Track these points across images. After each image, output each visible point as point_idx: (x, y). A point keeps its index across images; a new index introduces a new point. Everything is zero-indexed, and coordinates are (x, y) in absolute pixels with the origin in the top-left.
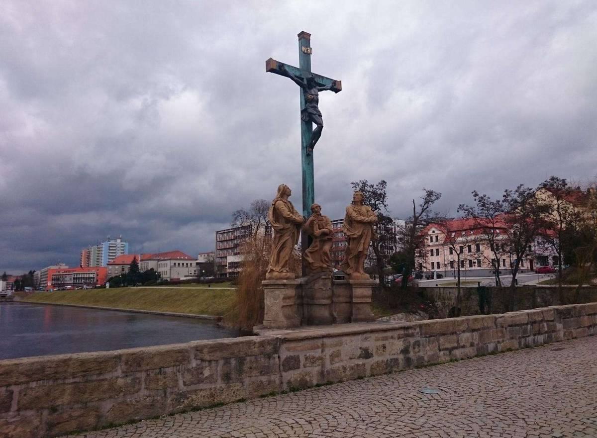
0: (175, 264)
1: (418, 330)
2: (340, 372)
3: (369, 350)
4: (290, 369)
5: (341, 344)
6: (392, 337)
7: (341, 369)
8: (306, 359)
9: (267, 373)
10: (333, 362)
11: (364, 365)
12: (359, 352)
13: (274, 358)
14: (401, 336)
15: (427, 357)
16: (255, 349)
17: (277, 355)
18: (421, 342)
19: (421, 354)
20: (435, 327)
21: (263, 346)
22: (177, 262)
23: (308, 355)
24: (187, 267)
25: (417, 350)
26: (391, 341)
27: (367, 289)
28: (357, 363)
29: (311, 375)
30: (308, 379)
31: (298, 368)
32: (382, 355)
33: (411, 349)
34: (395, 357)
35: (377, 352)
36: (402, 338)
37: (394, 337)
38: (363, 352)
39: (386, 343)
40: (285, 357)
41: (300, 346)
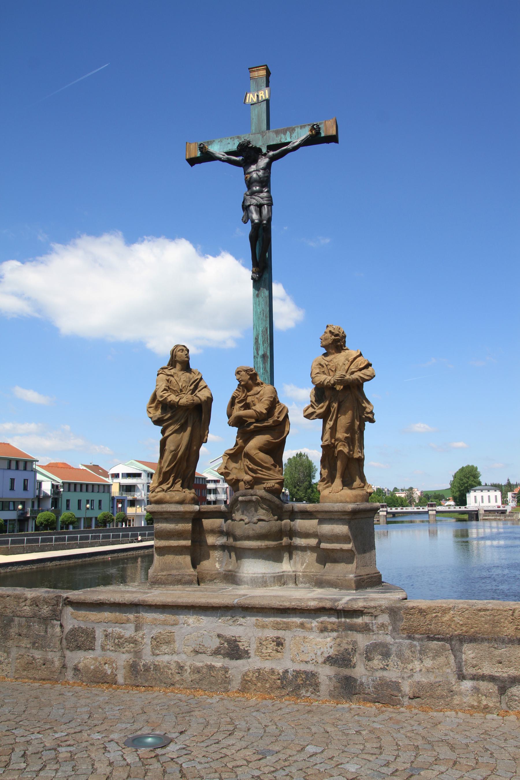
1: (384, 619)
2: (170, 671)
3: (240, 644)
4: (79, 648)
7: (173, 666)
9: (42, 647)
10: (157, 652)
11: (226, 670)
12: (216, 643)
14: (329, 627)
15: (411, 686)
16: (25, 608)
17: (59, 622)
18: (394, 649)
19: (392, 675)
20: (446, 618)
21: (37, 606)
23: (110, 630)
25: (377, 662)
28: (209, 663)
29: (114, 665)
30: (109, 672)
31: (92, 649)
32: (268, 657)
33: (356, 659)
34: (309, 668)
35: (258, 650)
36: (332, 630)
40: (71, 626)
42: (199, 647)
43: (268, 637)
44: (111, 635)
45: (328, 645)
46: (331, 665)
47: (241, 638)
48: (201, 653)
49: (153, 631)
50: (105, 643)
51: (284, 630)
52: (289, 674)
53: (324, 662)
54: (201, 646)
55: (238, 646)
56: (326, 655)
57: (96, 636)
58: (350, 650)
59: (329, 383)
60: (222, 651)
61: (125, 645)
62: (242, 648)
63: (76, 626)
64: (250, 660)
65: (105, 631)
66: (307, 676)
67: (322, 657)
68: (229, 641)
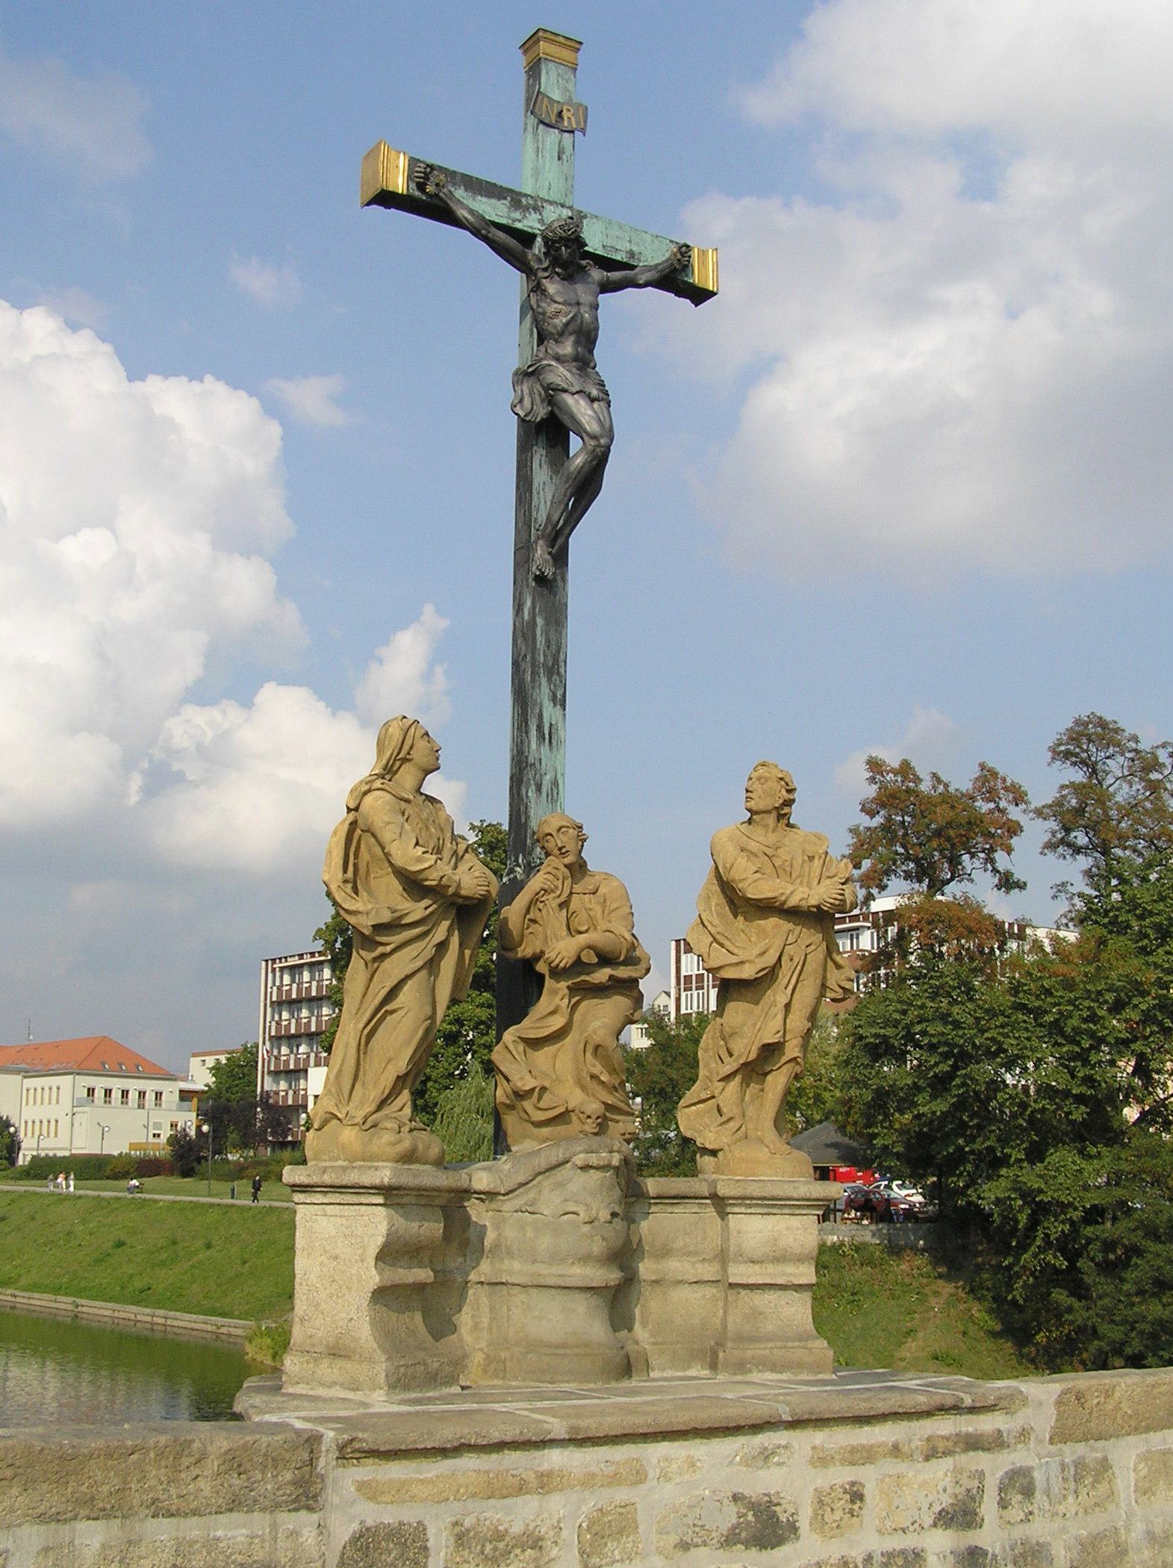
0: (91, 1092)
3: (778, 1509)
5: (639, 1476)
6: (896, 1450)
8: (461, 1539)
12: (729, 1516)
13: (294, 1534)
14: (941, 1446)
15: (1068, 1548)
17: (314, 1517)
22: (100, 1083)
24: (141, 1106)
26: (891, 1466)
27: (795, 1222)
33: (988, 1508)
35: (819, 1521)
36: (946, 1453)
37: (905, 1449)
38: (750, 1517)
39: (869, 1476)
40: (355, 1526)
41: (431, 1481)
42: (694, 1532)
43: (835, 1485)
44: (472, 1534)
45: (940, 1488)
46: (946, 1528)
47: (782, 1495)
48: (697, 1546)
49: (584, 1508)
50: (458, 1559)
51: (863, 1464)
52: (874, 1562)
53: (935, 1525)
54: (697, 1529)
55: (774, 1514)
56: (937, 1508)
57: (429, 1544)
58: (974, 1491)
59: (803, 903)
60: (743, 1535)
61: (512, 1555)
62: (783, 1518)
63: (369, 1523)
64: (798, 1545)
65: (456, 1524)
66: (906, 1559)
67: (931, 1514)
68: (753, 1506)
